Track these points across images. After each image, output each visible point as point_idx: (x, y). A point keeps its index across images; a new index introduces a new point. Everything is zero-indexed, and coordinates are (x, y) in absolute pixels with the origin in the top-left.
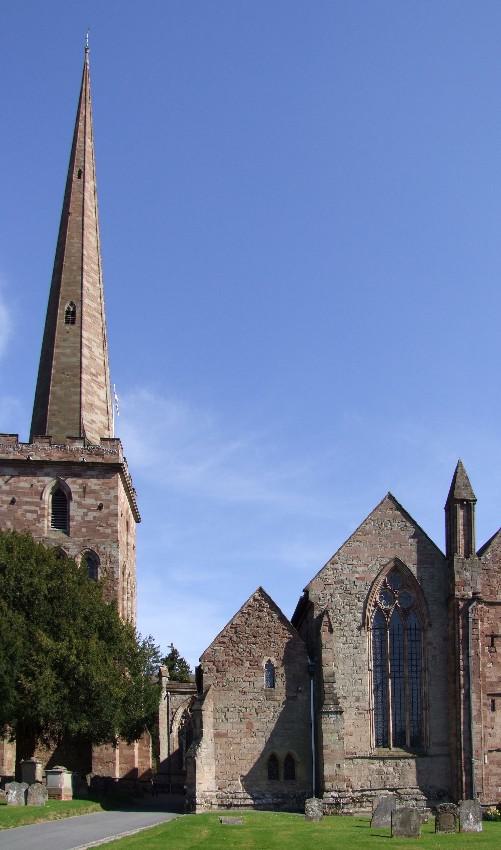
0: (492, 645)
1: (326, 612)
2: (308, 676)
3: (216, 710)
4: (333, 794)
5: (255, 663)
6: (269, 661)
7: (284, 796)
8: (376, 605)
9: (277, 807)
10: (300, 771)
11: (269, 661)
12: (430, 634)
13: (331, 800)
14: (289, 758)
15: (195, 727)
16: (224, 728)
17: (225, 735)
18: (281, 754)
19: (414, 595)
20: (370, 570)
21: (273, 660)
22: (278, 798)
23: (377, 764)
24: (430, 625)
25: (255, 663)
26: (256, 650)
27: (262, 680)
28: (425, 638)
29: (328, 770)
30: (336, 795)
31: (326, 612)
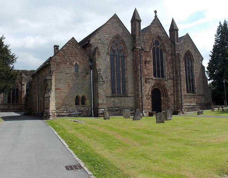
0: (146, 64)
1: (97, 48)
2: (90, 69)
3: (56, 79)
4: (102, 109)
5: (71, 64)
6: (76, 63)
7: (82, 111)
8: (111, 48)
9: (80, 115)
10: (87, 102)
11: (76, 63)
12: (128, 58)
13: (101, 112)
14: (83, 97)
15: (48, 86)
16: (58, 86)
17: (60, 89)
18: (81, 96)
19: (123, 46)
20: (107, 37)
21: (78, 63)
22: (80, 112)
23: (112, 99)
24: (128, 56)
25: (71, 64)
26: (72, 59)
27: (73, 70)
28: (126, 59)
29: (100, 101)
30: (103, 110)
31: (97, 48)
